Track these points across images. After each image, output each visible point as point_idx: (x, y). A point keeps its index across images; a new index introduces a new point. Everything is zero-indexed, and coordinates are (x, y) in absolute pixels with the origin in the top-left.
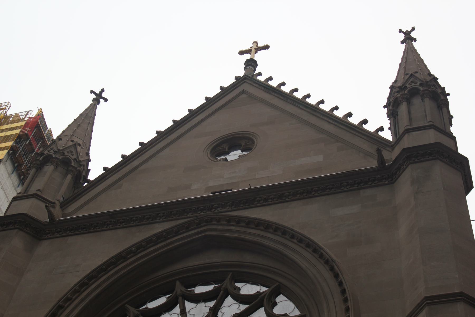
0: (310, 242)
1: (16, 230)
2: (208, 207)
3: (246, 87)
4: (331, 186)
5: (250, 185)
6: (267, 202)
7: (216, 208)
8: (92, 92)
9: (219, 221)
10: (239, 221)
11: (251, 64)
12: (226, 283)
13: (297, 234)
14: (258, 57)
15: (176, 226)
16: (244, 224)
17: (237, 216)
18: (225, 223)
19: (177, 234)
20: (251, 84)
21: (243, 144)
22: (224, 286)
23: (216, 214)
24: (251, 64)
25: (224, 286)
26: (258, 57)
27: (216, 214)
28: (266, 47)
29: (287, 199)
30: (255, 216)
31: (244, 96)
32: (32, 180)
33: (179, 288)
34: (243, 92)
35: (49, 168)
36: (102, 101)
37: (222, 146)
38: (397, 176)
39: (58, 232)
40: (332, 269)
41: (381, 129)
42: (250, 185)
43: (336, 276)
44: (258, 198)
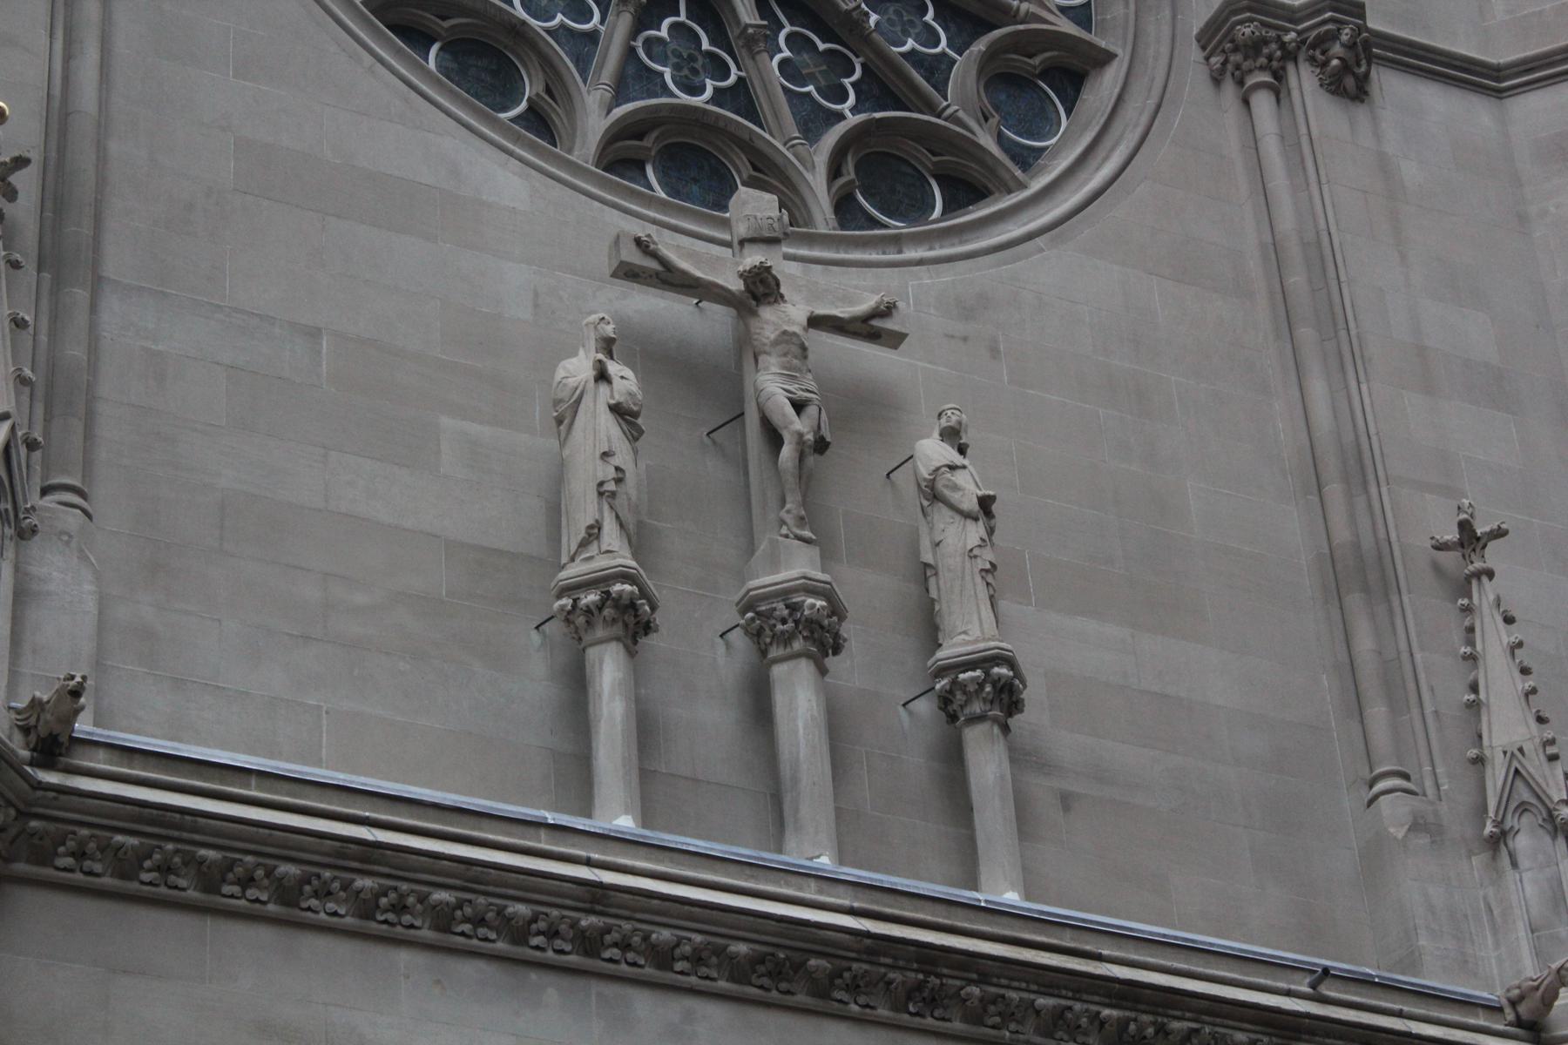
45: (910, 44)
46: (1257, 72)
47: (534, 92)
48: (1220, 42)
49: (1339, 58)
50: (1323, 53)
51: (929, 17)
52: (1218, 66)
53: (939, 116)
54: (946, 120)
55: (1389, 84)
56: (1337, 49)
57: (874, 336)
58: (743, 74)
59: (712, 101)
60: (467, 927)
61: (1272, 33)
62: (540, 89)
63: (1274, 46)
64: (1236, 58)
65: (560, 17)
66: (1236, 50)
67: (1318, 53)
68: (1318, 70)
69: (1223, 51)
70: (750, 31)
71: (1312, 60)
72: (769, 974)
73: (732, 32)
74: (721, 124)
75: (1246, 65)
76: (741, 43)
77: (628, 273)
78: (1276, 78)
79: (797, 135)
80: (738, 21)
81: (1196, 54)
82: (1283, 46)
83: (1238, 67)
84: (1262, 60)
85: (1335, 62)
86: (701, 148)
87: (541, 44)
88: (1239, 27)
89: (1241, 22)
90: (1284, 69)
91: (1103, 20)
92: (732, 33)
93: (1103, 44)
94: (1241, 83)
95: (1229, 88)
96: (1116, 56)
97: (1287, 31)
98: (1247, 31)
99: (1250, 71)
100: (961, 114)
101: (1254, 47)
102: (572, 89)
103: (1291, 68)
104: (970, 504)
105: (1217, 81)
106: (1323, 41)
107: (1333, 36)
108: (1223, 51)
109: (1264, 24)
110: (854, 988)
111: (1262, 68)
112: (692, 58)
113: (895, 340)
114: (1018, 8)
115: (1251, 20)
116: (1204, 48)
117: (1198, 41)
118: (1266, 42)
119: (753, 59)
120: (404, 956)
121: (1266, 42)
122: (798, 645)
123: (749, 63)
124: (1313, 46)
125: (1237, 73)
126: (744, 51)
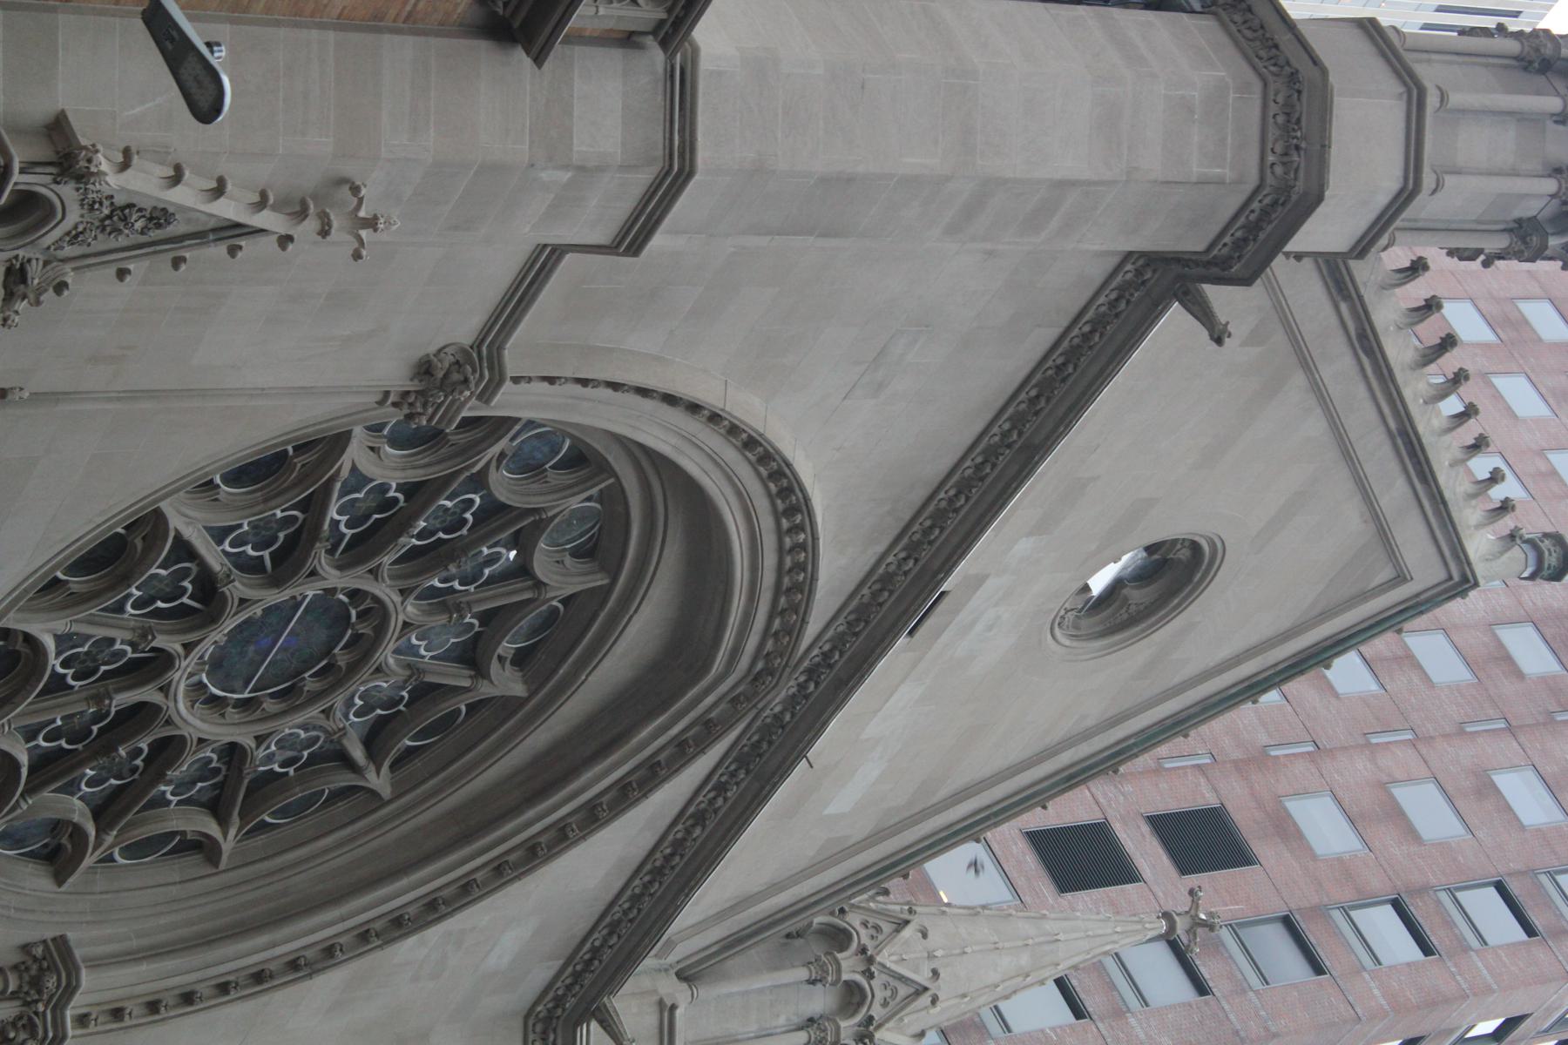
0: (436, 916)
2: (822, 673)
4: (631, 916)
5: (812, 767)
6: (882, 575)
7: (802, 687)
9: (735, 701)
10: (683, 751)
13: (498, 884)
15: (804, 622)
16: (662, 757)
17: (703, 751)
18: (713, 715)
20: (1417, 595)
23: (760, 706)
27: (760, 706)
29: (680, 827)
38: (531, 1037)
39: (1113, 304)
42: (812, 767)
43: (260, 977)
44: (742, 776)
45: (246, 528)
46: (18, 983)
47: (71, 585)
48: (52, 956)
49: (14, 1038)
50: (24, 1026)
51: (113, 781)
52: (34, 952)
53: (22, 795)
54: (17, 801)
56: (23, 1036)
58: (76, 688)
59: (54, 674)
61: (45, 997)
62: (75, 588)
63: (36, 997)
64: (33, 972)
65: (59, 722)
66: (41, 969)
67: (24, 1021)
68: (11, 1020)
69: (44, 959)
70: (107, 702)
71: (20, 1017)
73: (112, 684)
74: (28, 688)
75: (26, 978)
76: (102, 690)
78: (12, 993)
79: (72, 630)
80: (119, 690)
81: (49, 934)
82: (36, 1002)
83: (27, 969)
84: (26, 989)
85: (12, 1035)
86: (14, 668)
87: (109, 595)
88: (55, 978)
89: (59, 980)
90: (18, 998)
91: (96, 873)
92: (111, 684)
93: (71, 880)
94: (15, 968)
95: (16, 958)
96: (60, 883)
97: (46, 1007)
98: (50, 985)
99: (21, 978)
100: (19, 811)
101: (36, 983)
102: (68, 612)
103: (18, 1003)
105: (26, 948)
106: (31, 1027)
108: (44, 959)
109: (52, 996)
111: (20, 987)
112: (95, 660)
114: (108, 834)
115: (58, 987)
116: (54, 940)
117: (61, 936)
119: (86, 699)
121: (39, 992)
123: (84, 694)
124: (30, 1019)
125: (23, 967)
126: (94, 691)
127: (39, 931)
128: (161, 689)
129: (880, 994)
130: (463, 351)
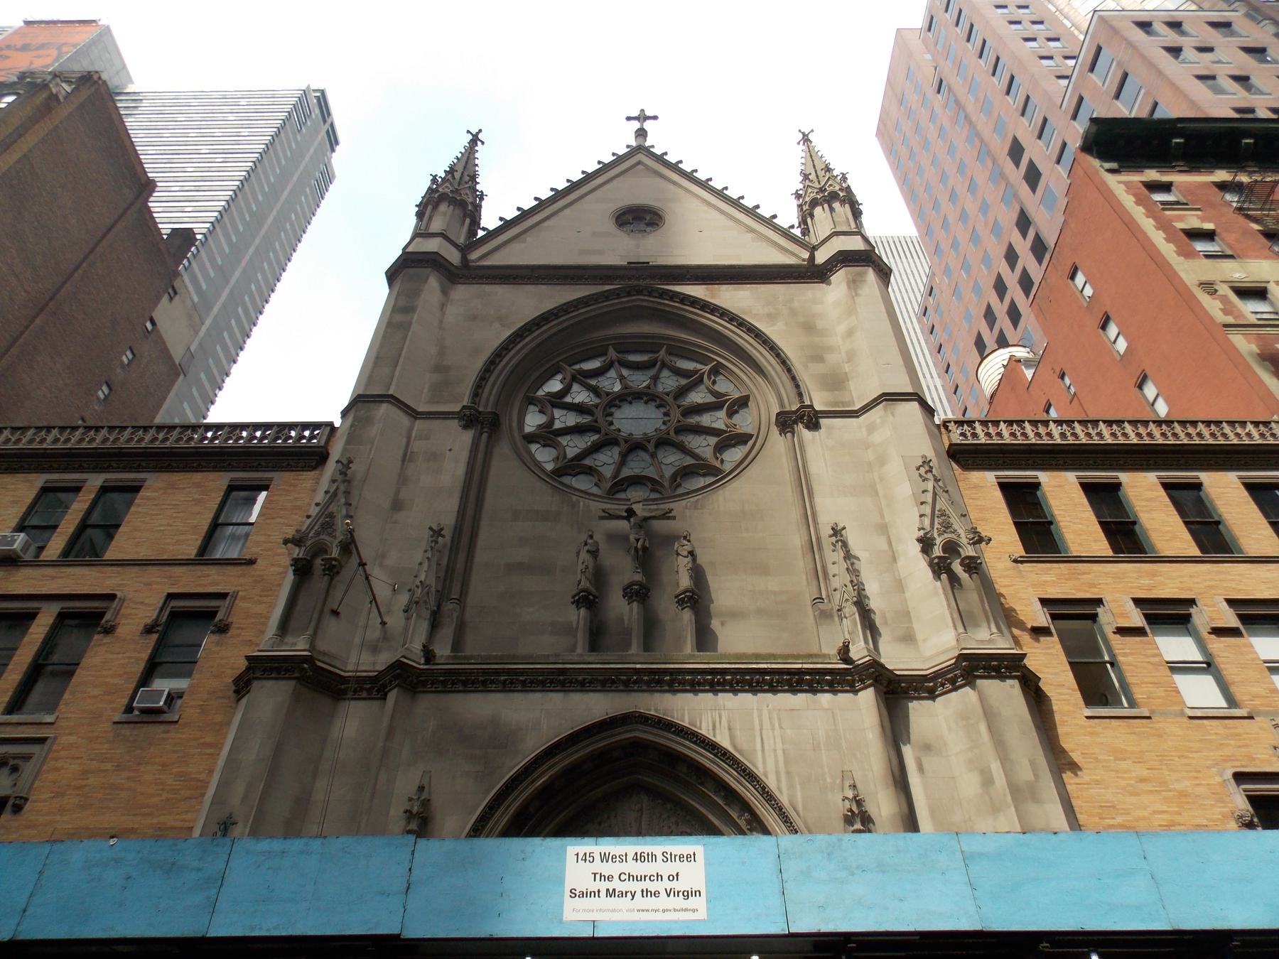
1: (430, 269)
3: (641, 157)
8: (468, 132)
11: (641, 133)
12: (662, 353)
14: (648, 125)
17: (671, 291)
19: (607, 299)
21: (648, 218)
22: (661, 357)
24: (641, 133)
25: (661, 357)
26: (648, 125)
28: (655, 118)
30: (692, 294)
31: (640, 167)
32: (430, 218)
33: (612, 354)
34: (639, 163)
35: (443, 207)
36: (479, 143)
37: (627, 216)
40: (778, 355)
41: (792, 227)
55: (823, 422)
57: (668, 518)
60: (568, 685)
72: (611, 683)
77: (602, 518)
104: (686, 554)
107: (804, 415)
110: (636, 682)
113: (674, 518)
118: (786, 421)
120: (516, 695)
122: (634, 598)
127: (775, 431)
128: (649, 442)
129: (812, 195)
130: (459, 421)
